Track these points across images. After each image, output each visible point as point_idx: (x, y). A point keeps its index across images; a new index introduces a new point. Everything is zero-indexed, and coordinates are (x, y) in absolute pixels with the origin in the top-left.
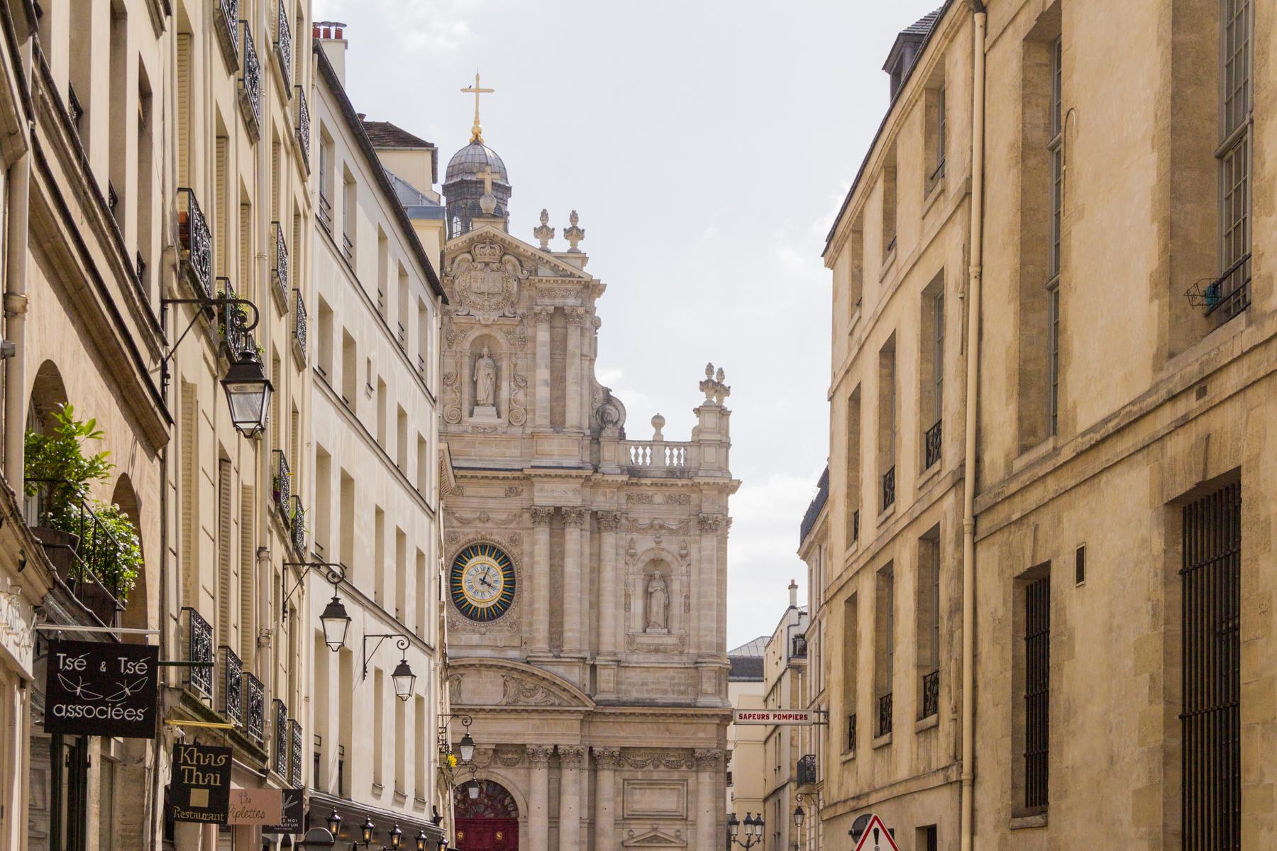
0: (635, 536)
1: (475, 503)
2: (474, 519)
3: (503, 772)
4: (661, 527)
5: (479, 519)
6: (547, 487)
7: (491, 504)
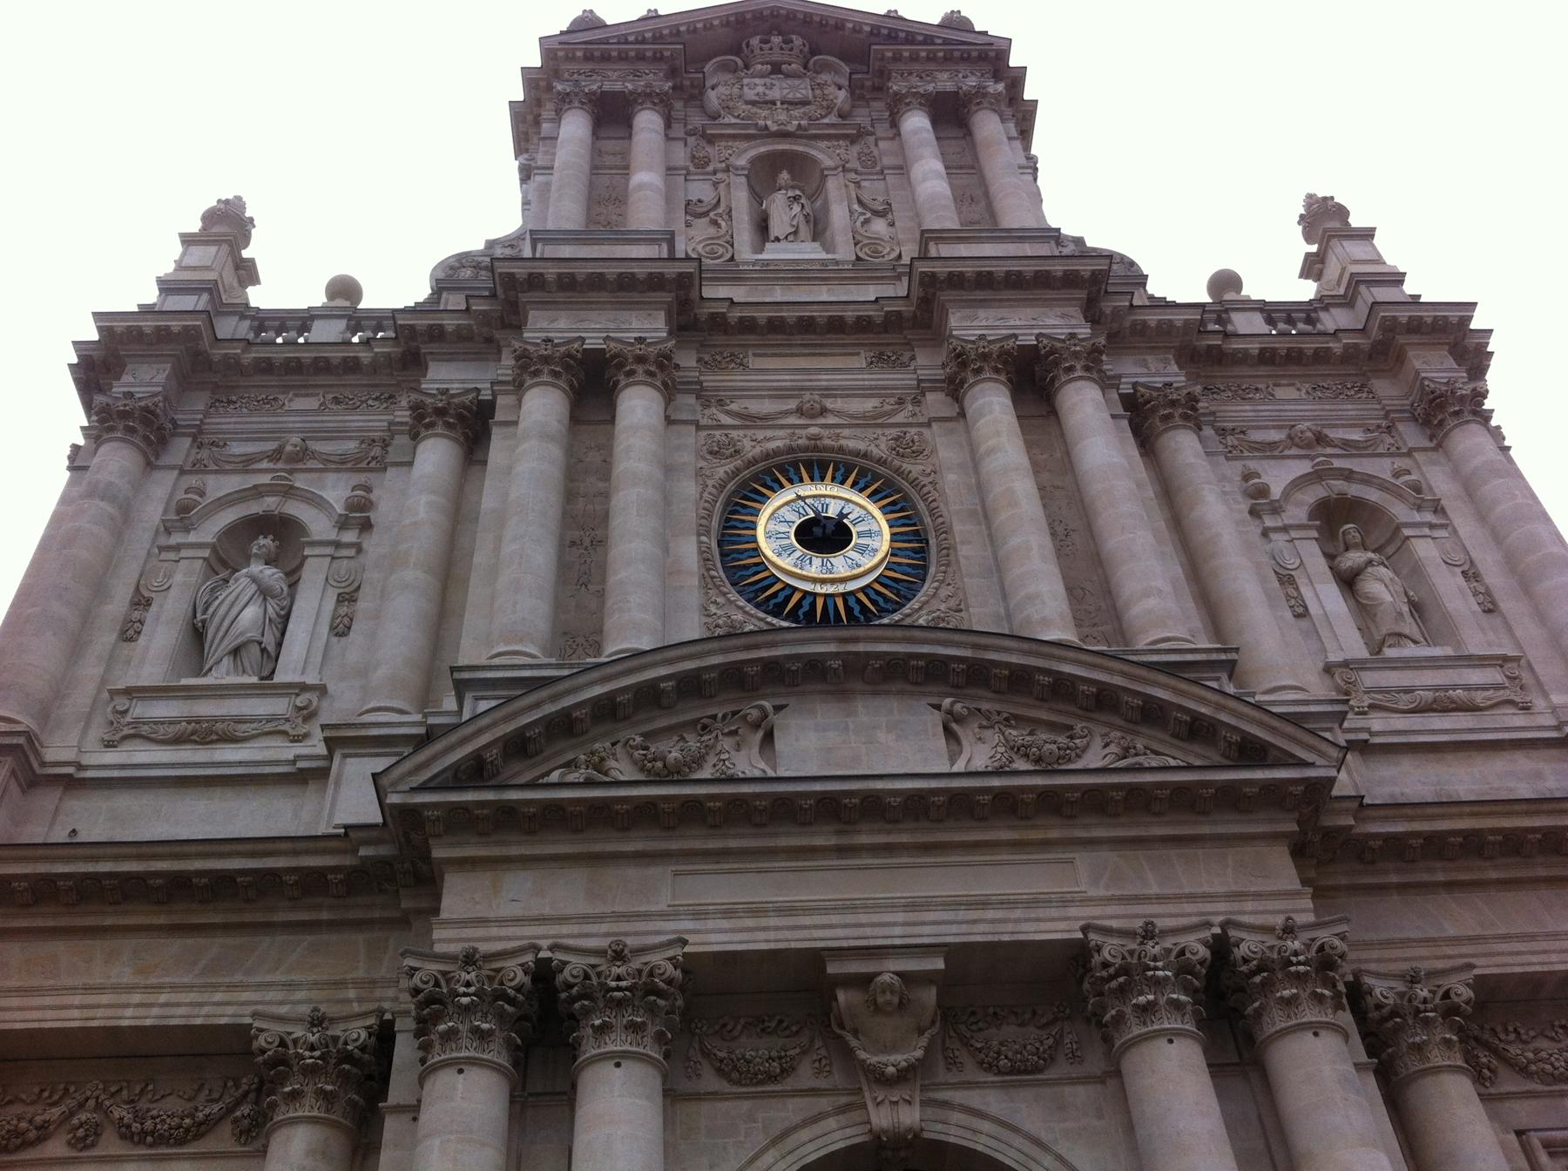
0: (1253, 465)
1: (786, 380)
2: (787, 413)
3: (992, 1101)
4: (1320, 439)
5: (800, 411)
6: (982, 313)
7: (824, 380)
